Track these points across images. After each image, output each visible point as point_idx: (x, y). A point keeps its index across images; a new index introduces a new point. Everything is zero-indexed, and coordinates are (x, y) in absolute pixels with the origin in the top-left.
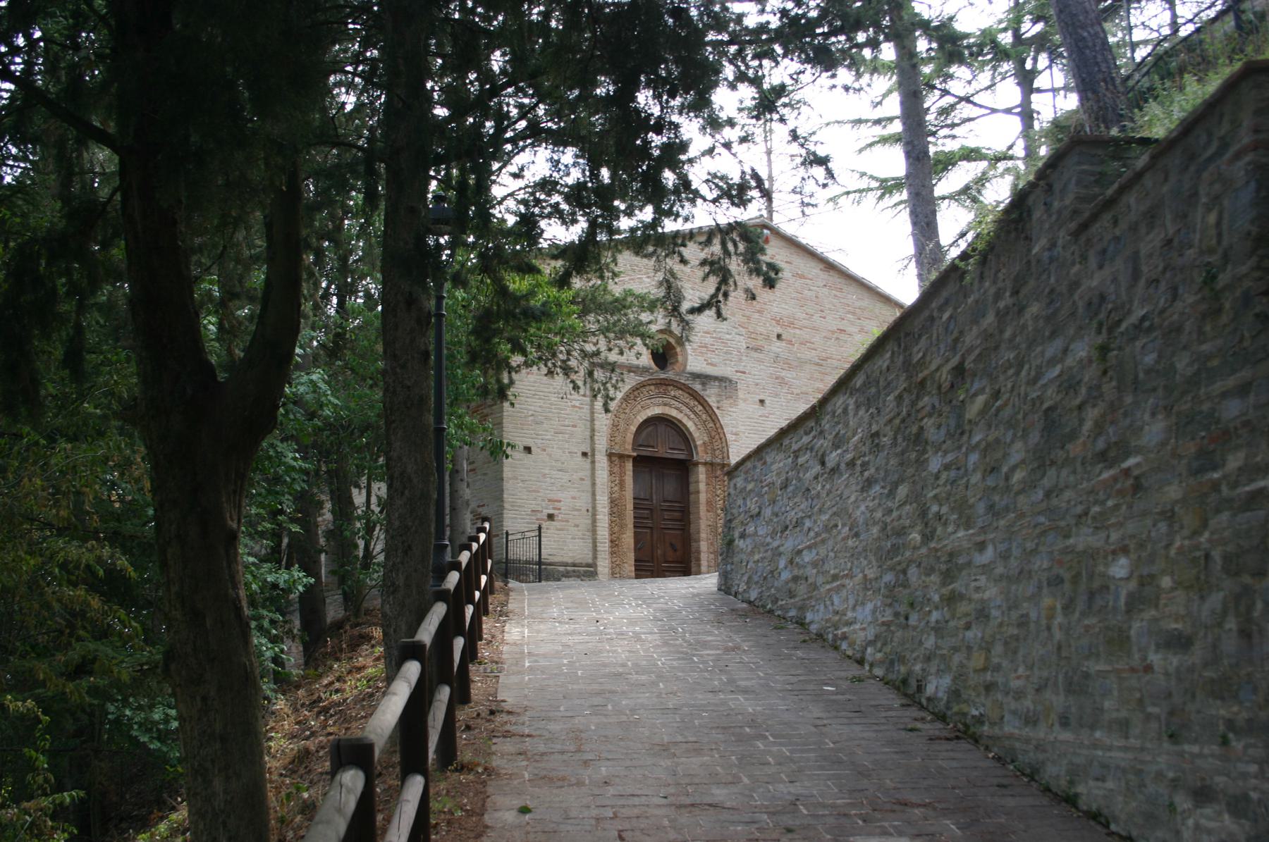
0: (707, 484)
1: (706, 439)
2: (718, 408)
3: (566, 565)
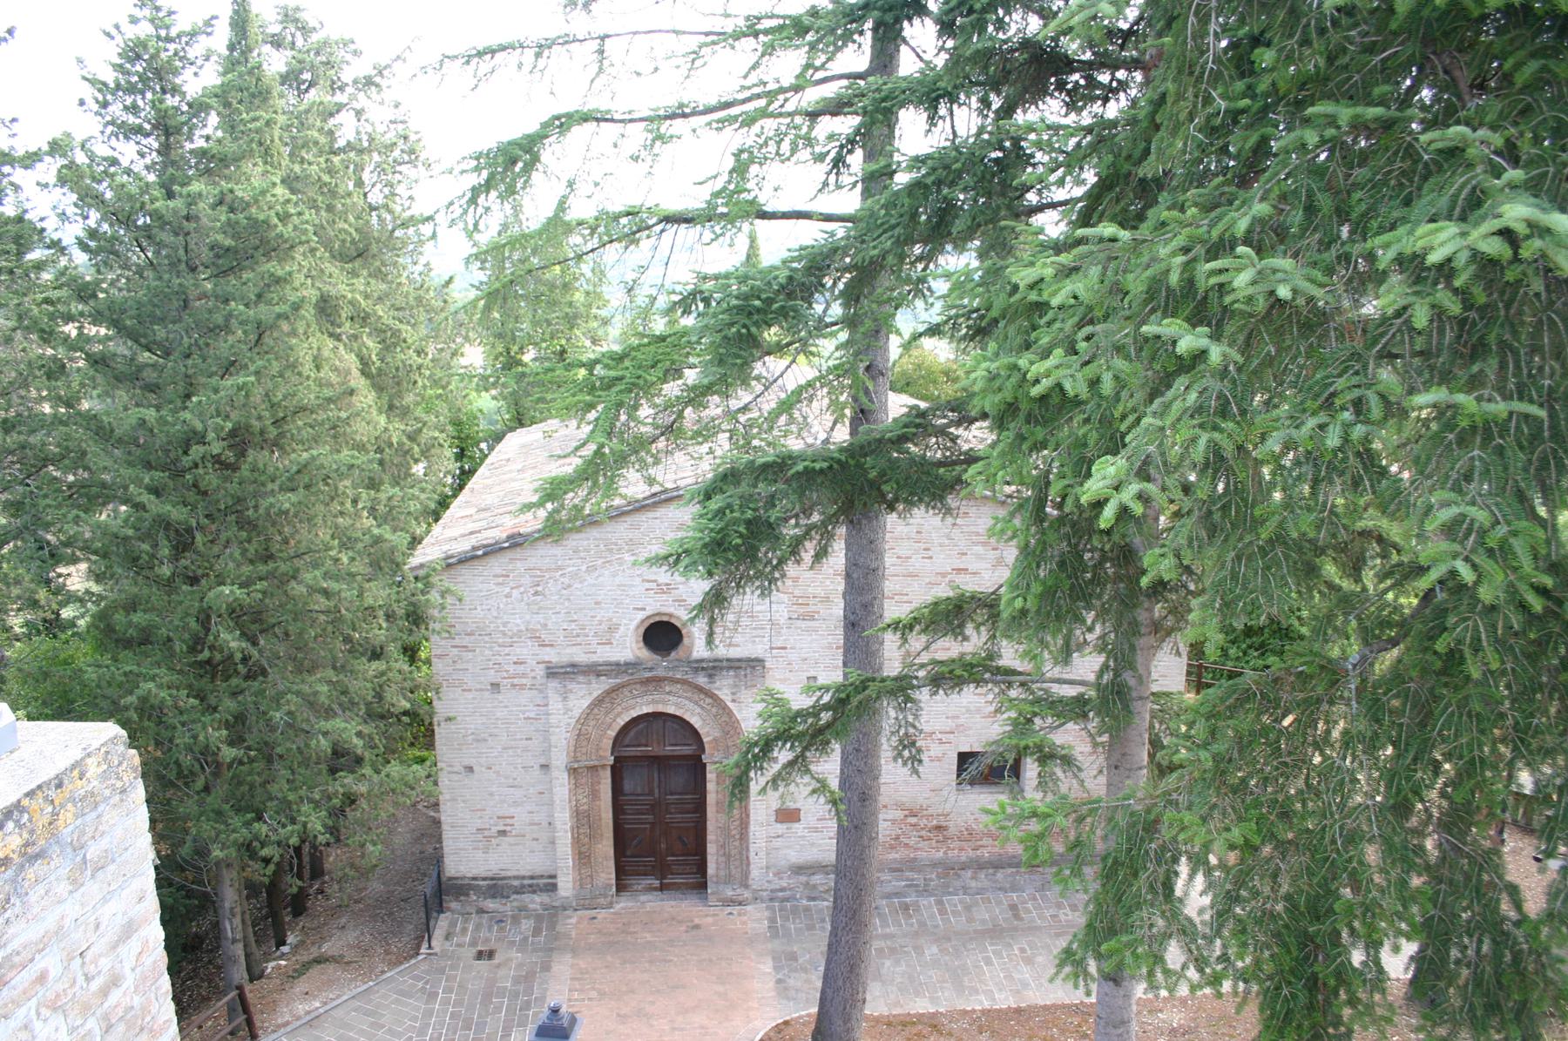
1: (717, 734)
3: (523, 878)
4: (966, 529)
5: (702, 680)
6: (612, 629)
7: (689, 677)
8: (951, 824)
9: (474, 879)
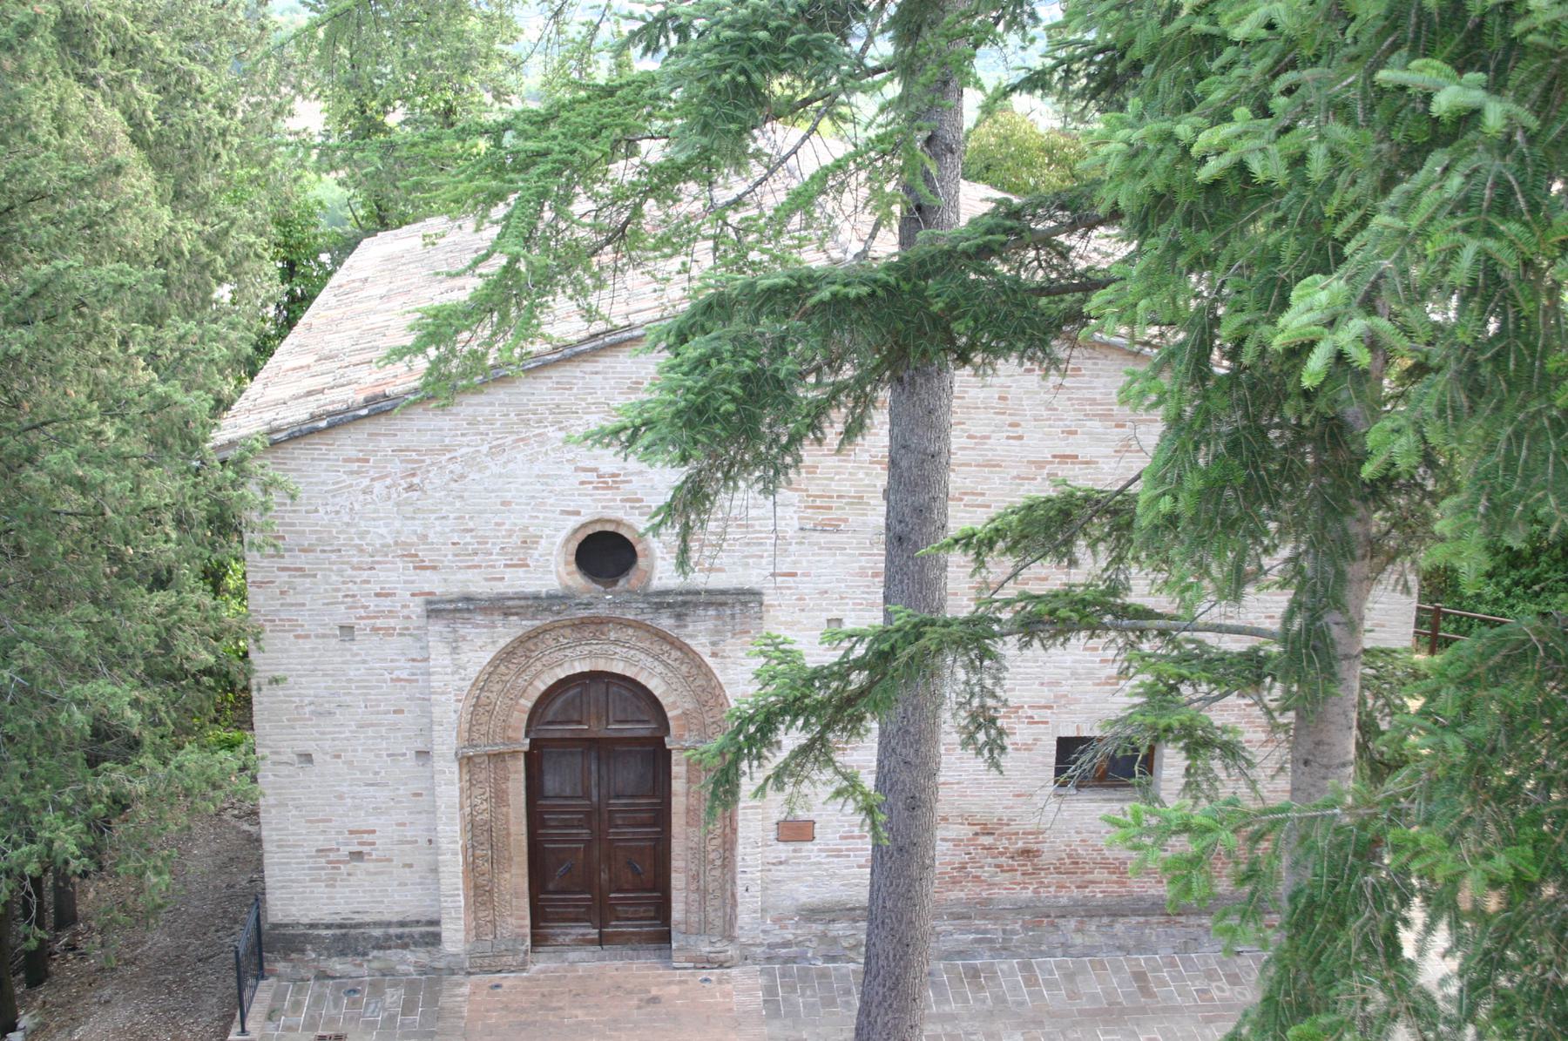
0: (689, 781)
2: (714, 655)
3: (389, 924)
4: (1079, 394)
5: (665, 622)
6: (528, 543)
7: (647, 618)
8: (1045, 847)
9: (312, 926)
